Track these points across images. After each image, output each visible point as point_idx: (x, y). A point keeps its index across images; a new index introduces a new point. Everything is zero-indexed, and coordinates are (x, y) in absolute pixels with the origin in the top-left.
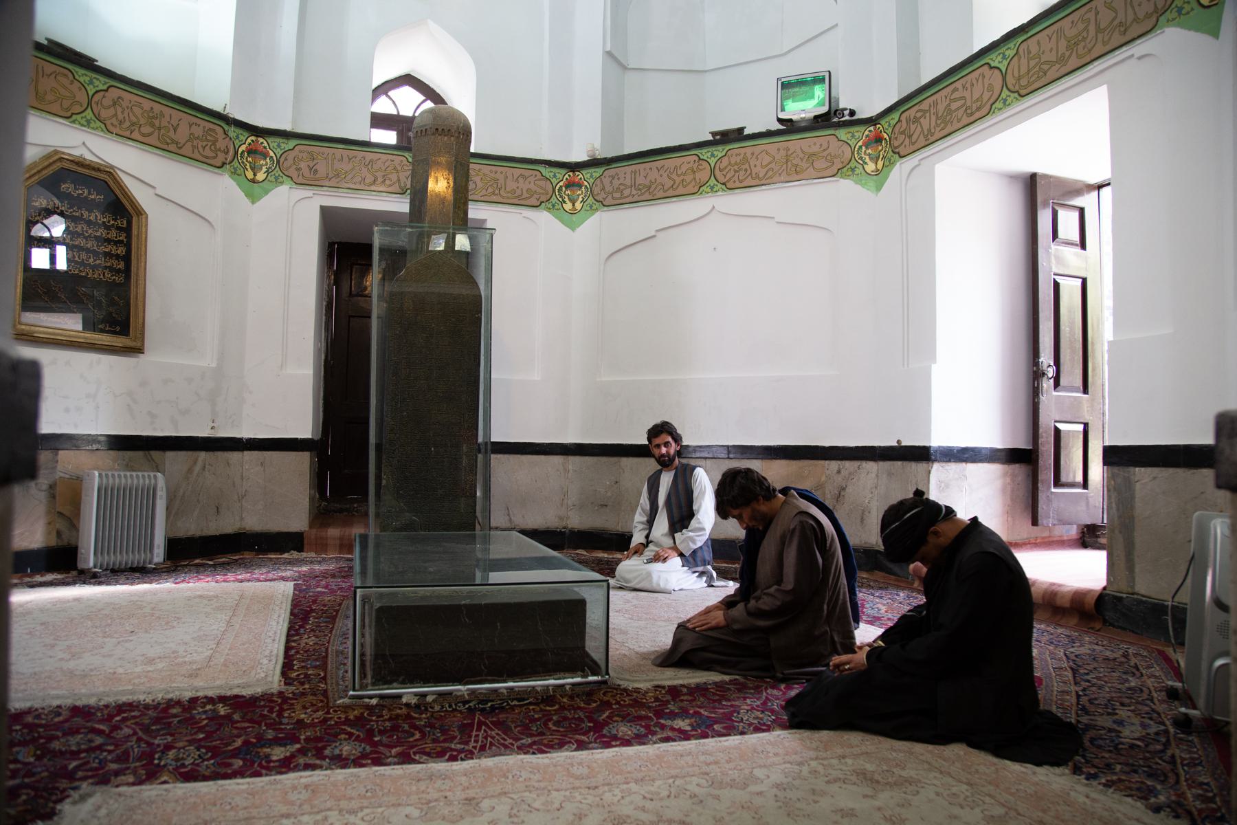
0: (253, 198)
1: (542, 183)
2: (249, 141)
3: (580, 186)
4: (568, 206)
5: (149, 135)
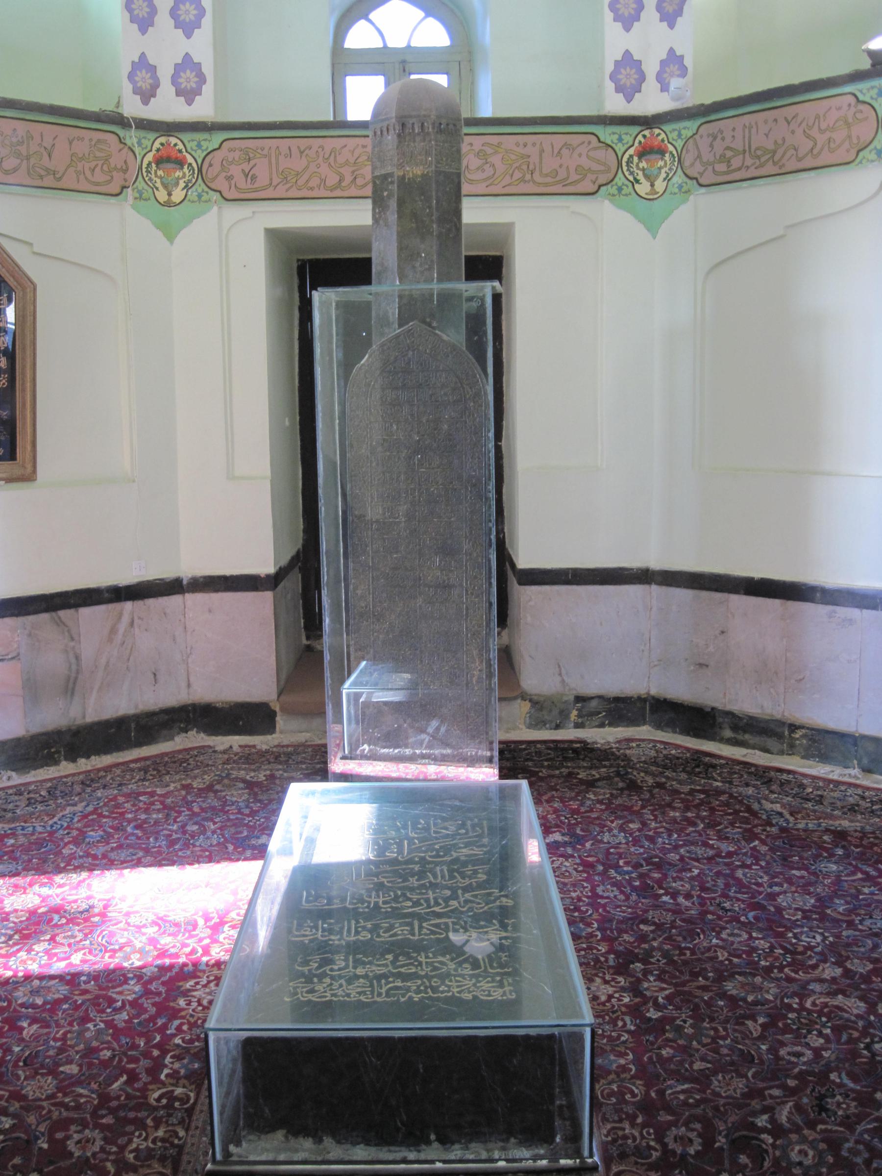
0: (170, 233)
1: (601, 154)
2: (157, 145)
3: (661, 151)
4: (643, 188)
5: (15, 170)
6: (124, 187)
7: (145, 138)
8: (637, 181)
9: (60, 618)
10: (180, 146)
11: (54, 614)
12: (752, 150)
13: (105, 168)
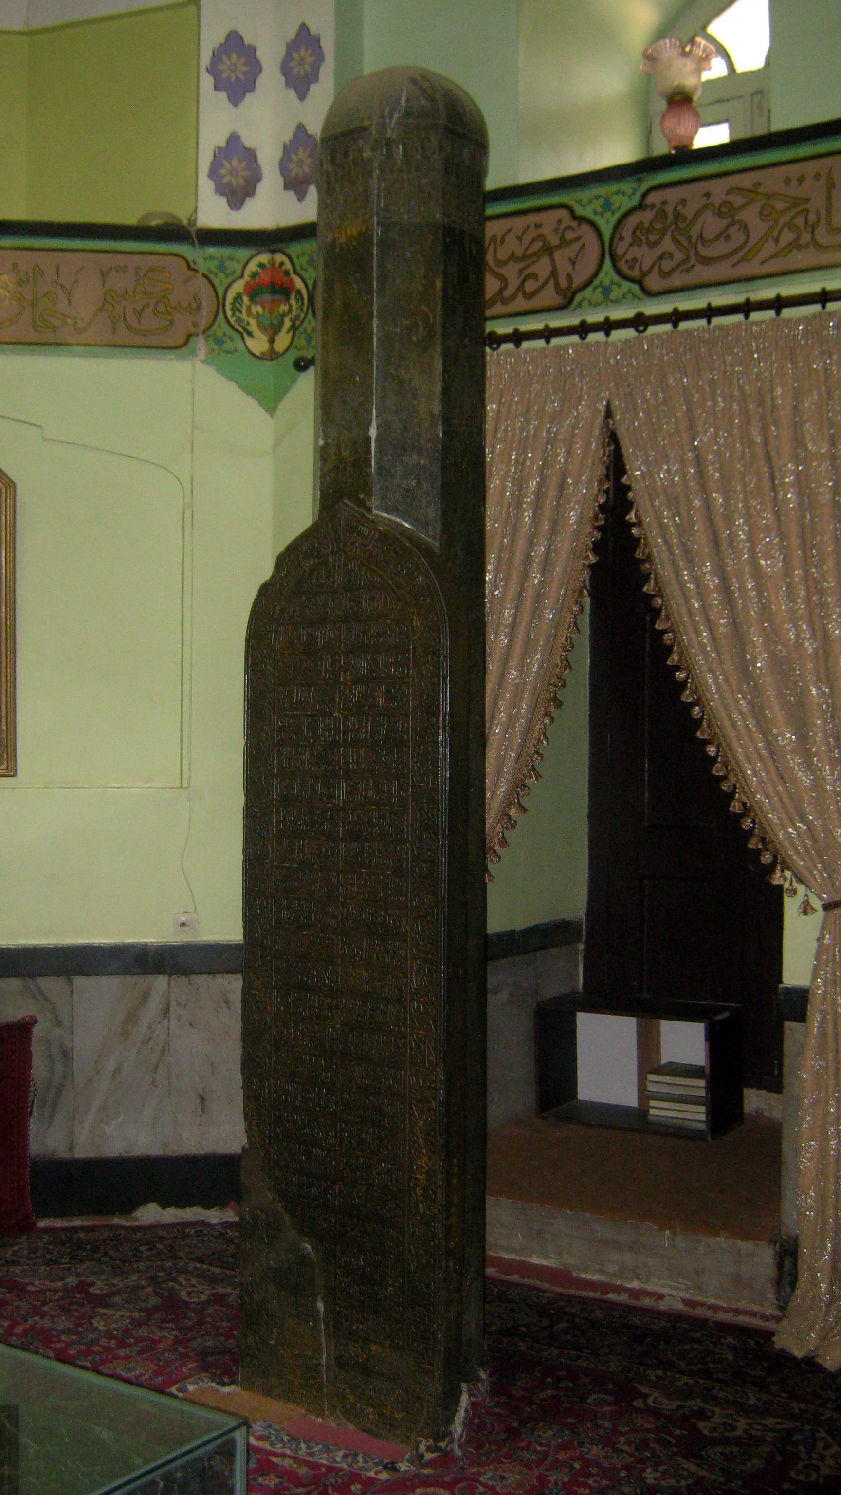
2: (252, 267)
6: (189, 336)
7: (231, 258)
9: (39, 988)
10: (288, 266)
11: (29, 981)
13: (162, 308)
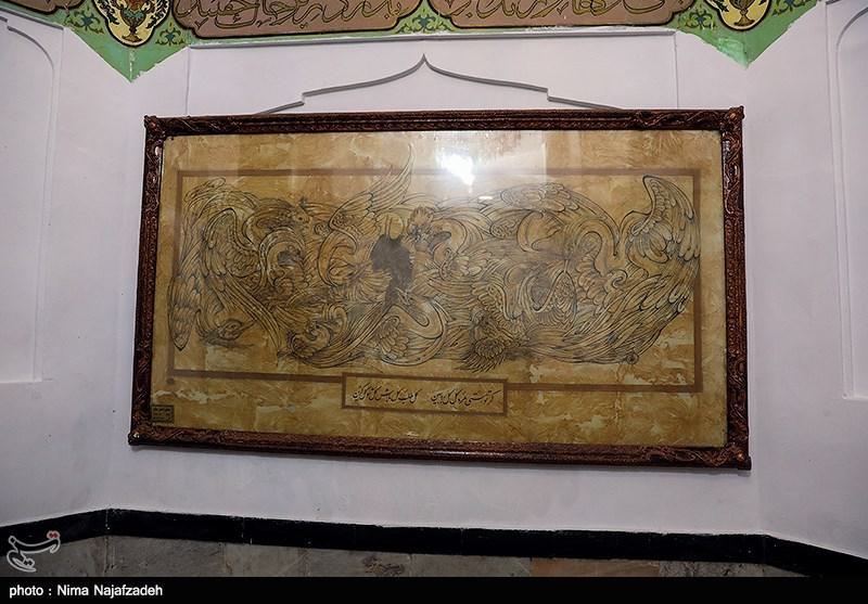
8: (114, 20)
12: (267, 6)
